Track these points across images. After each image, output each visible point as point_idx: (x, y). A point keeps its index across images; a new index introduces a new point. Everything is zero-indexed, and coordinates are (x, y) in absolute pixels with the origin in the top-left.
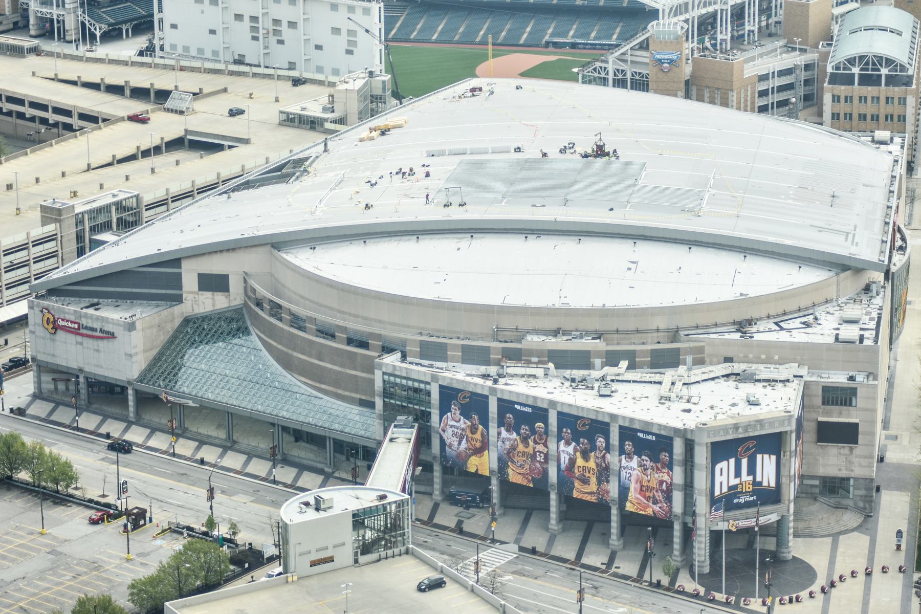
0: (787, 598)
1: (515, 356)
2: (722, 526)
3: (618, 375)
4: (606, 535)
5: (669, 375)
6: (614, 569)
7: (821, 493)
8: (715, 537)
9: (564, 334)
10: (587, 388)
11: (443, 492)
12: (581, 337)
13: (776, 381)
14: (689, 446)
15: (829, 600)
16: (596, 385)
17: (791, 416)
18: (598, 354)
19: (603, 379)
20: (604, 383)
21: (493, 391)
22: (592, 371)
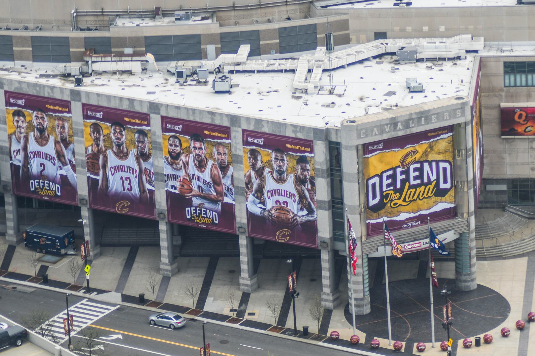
0: (473, 339)
1: (102, 47)
2: (383, 252)
3: (238, 64)
4: (235, 272)
5: (303, 60)
6: (247, 317)
7: (512, 202)
8: (376, 266)
9: (164, 15)
10: (199, 82)
11: (18, 231)
12: (187, 18)
13: (444, 59)
14: (335, 151)
15: (527, 338)
16: (211, 78)
17: (464, 104)
18: (211, 39)
19: (219, 70)
20: (220, 75)
21: (76, 95)
22: (204, 62)
